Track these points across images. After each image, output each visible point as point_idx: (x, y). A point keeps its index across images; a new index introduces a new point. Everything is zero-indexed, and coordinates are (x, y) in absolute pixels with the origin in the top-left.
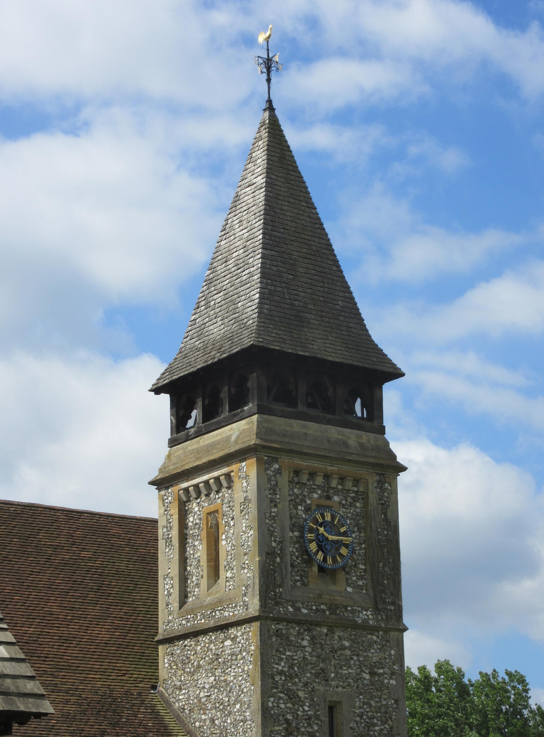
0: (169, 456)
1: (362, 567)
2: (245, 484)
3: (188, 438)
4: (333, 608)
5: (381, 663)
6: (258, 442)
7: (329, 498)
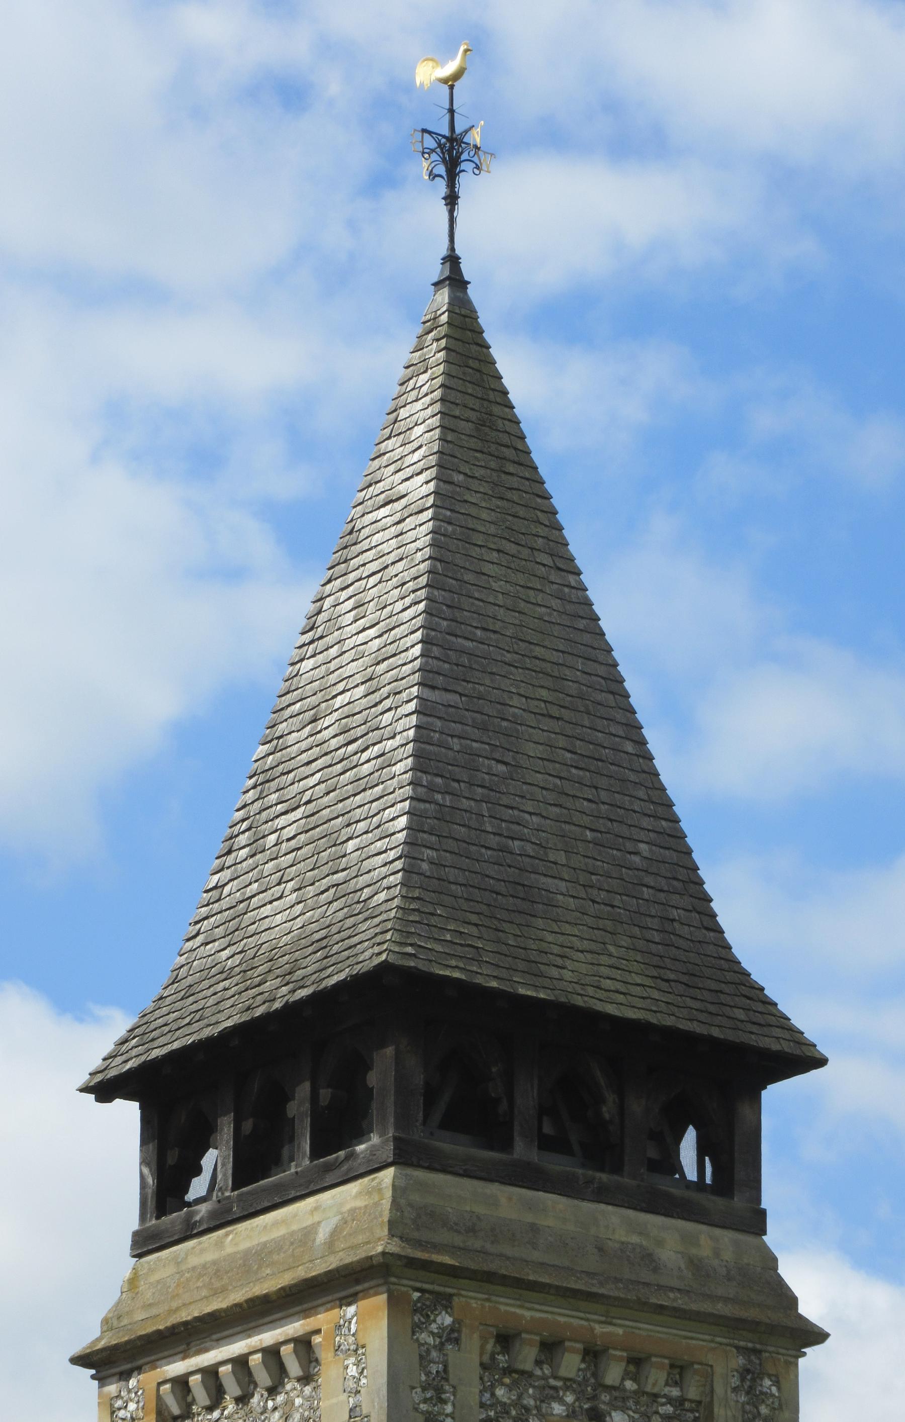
0: (133, 1282)
2: (353, 1371)
3: (189, 1232)
6: (395, 1247)
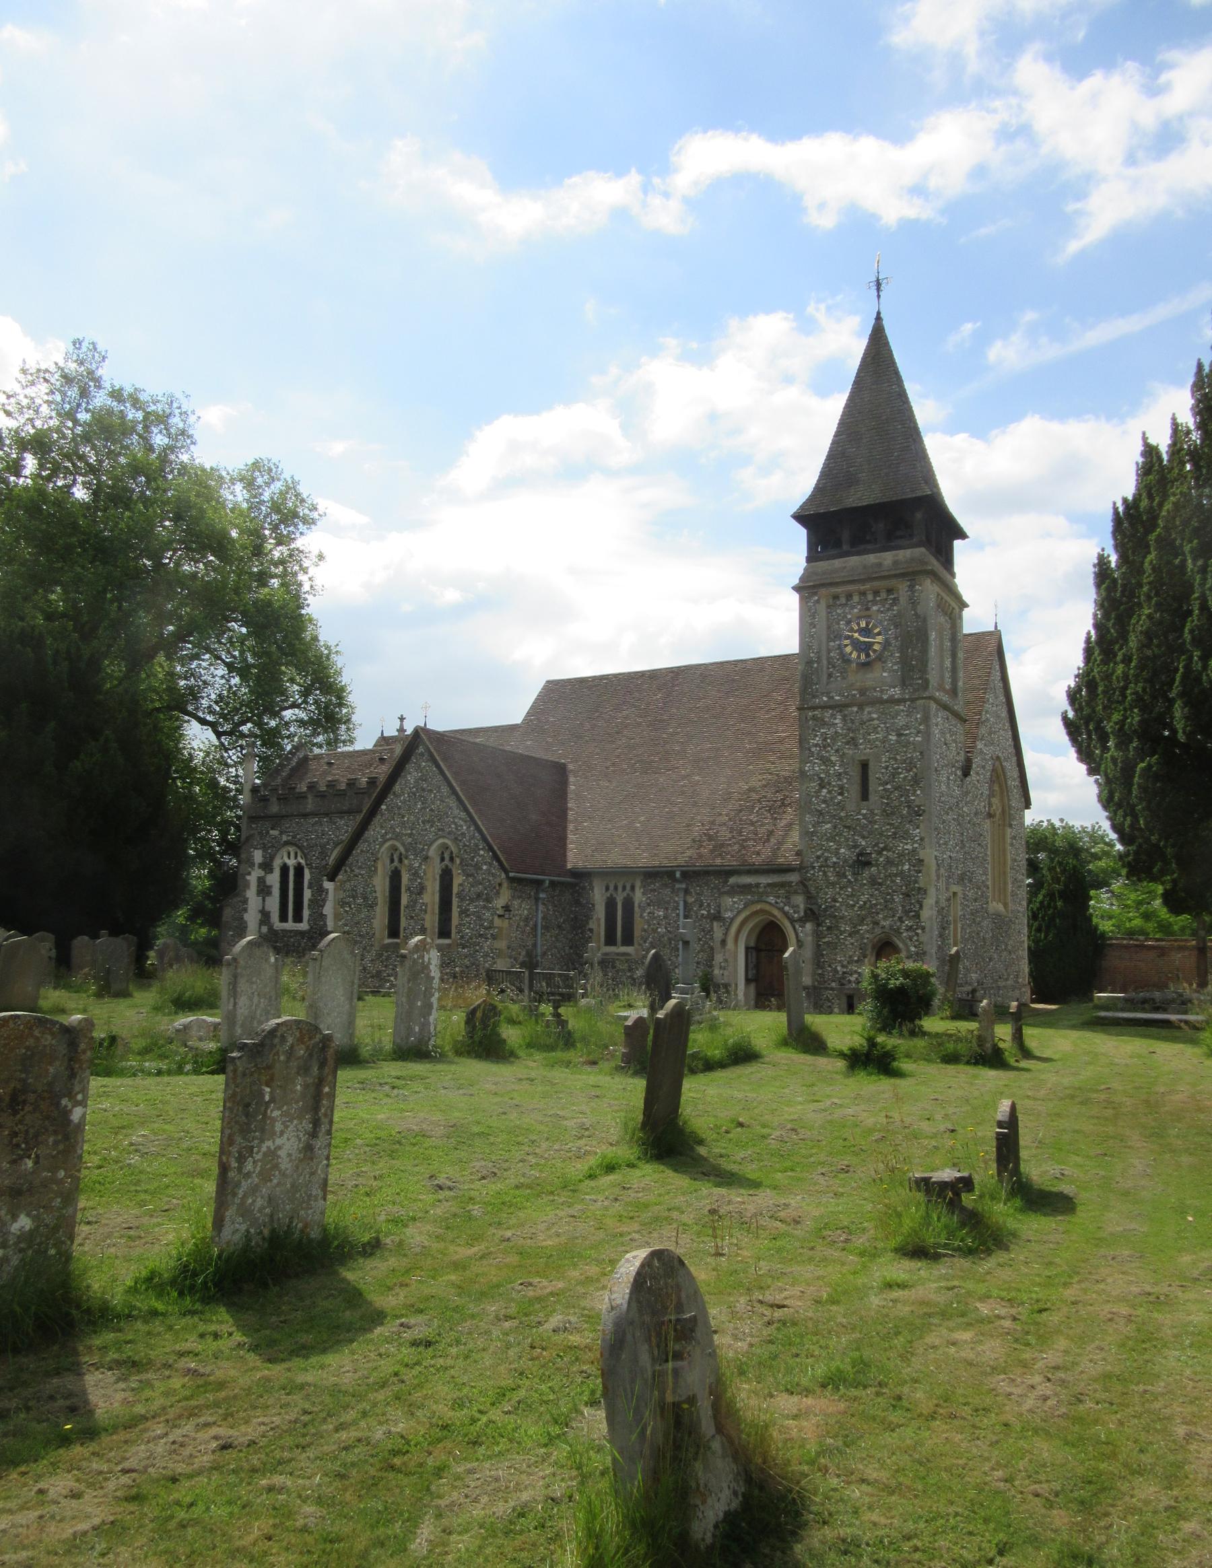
4: (863, 692)
7: (868, 609)
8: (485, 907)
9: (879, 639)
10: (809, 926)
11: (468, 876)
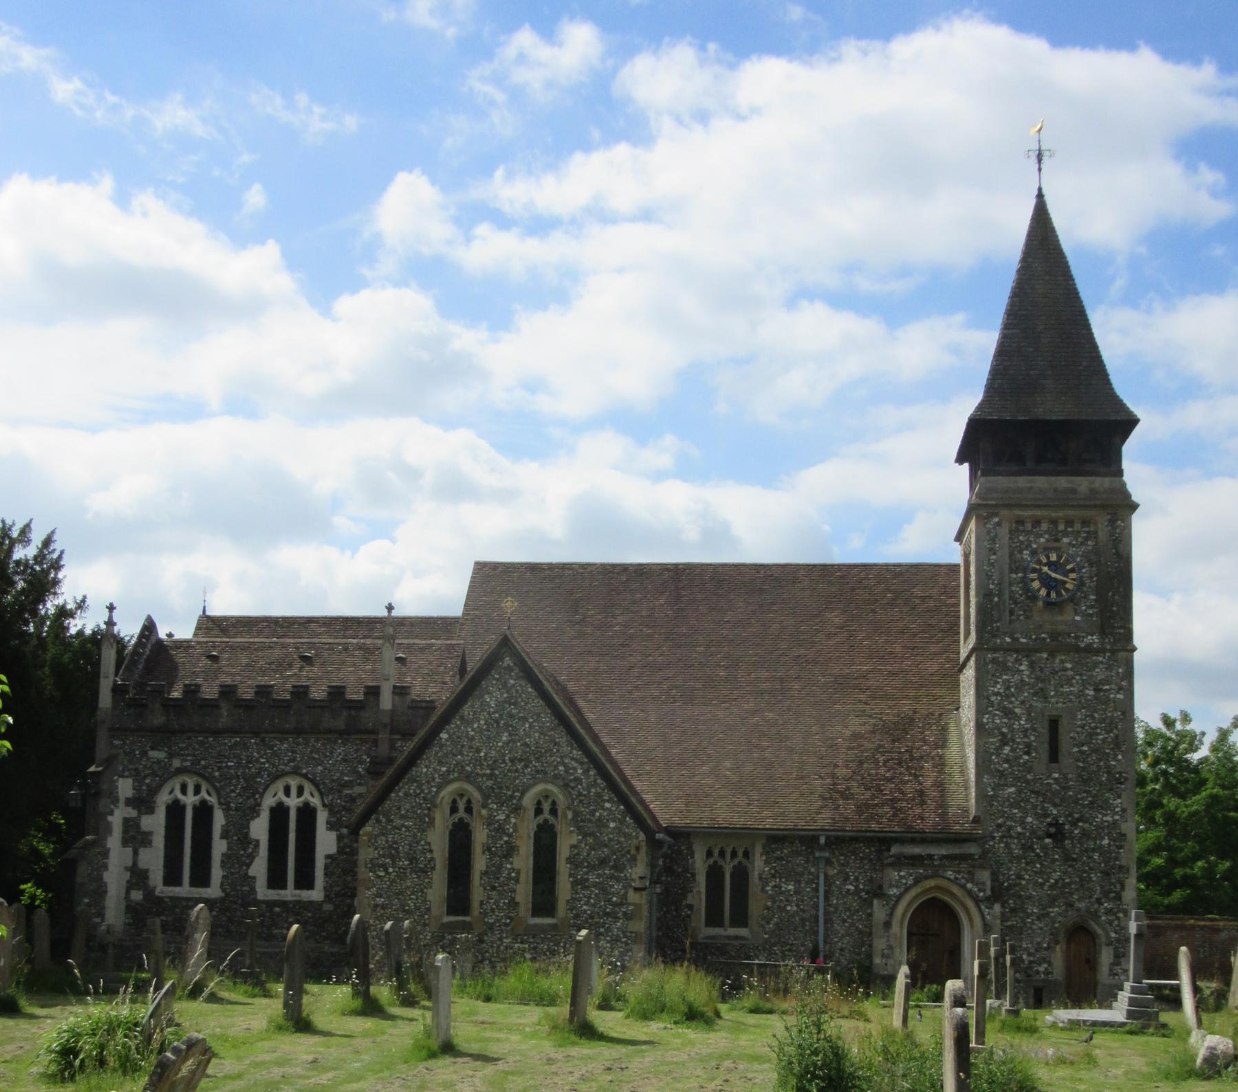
1: (1092, 597)
4: (1055, 636)
5: (1107, 681)
6: (980, 502)
7: (1057, 540)
8: (612, 877)
9: (1073, 575)
10: (997, 908)
11: (585, 835)
